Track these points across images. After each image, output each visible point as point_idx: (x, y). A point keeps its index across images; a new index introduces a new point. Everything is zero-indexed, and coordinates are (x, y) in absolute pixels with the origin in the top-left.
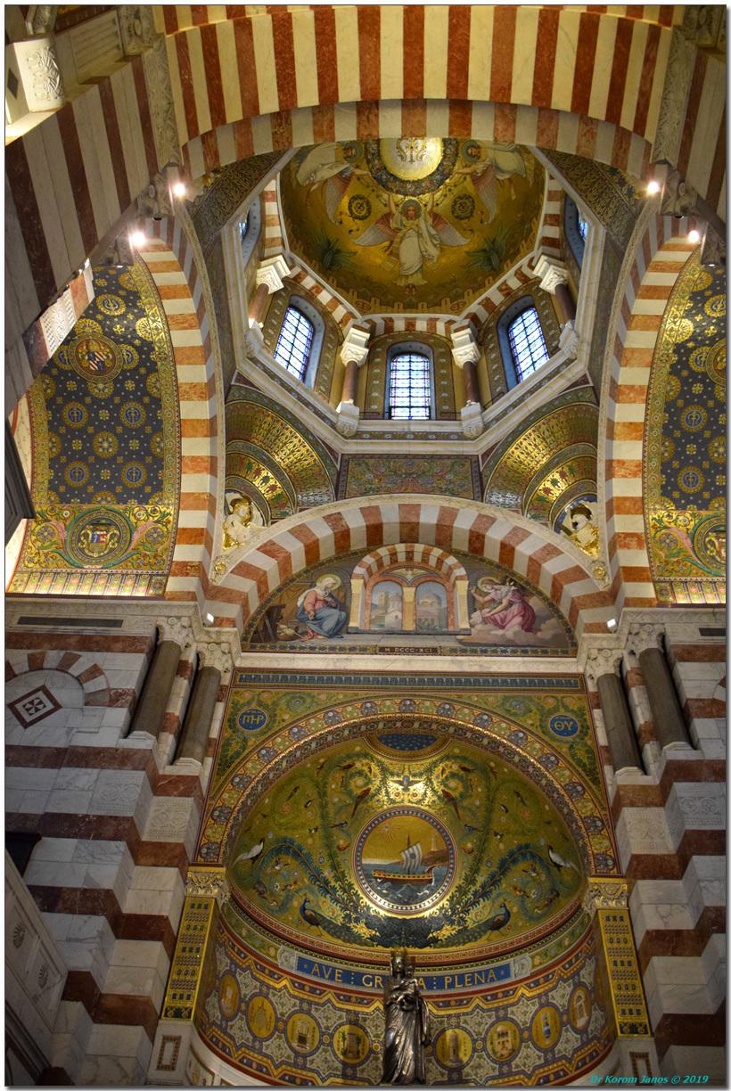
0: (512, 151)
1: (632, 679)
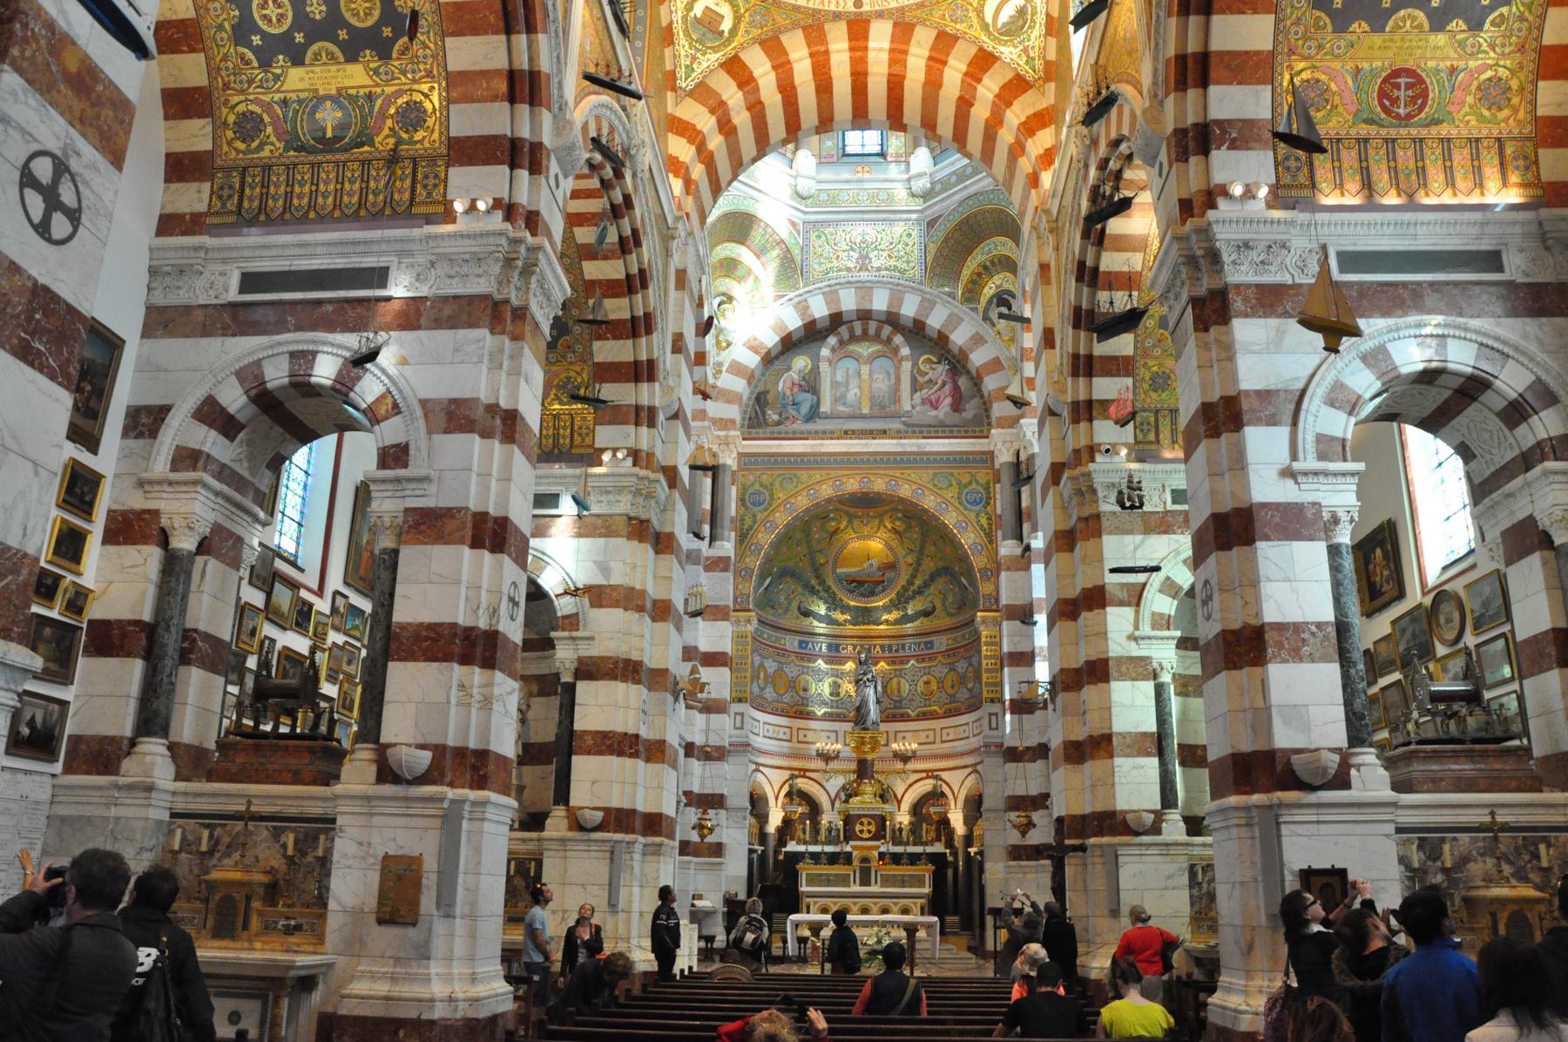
1: (1023, 467)
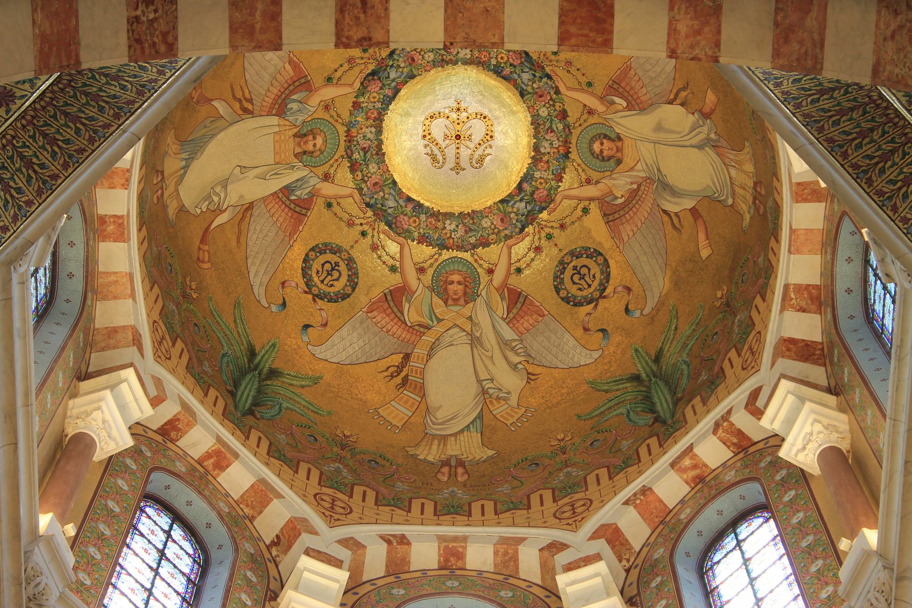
0: (700, 147)
